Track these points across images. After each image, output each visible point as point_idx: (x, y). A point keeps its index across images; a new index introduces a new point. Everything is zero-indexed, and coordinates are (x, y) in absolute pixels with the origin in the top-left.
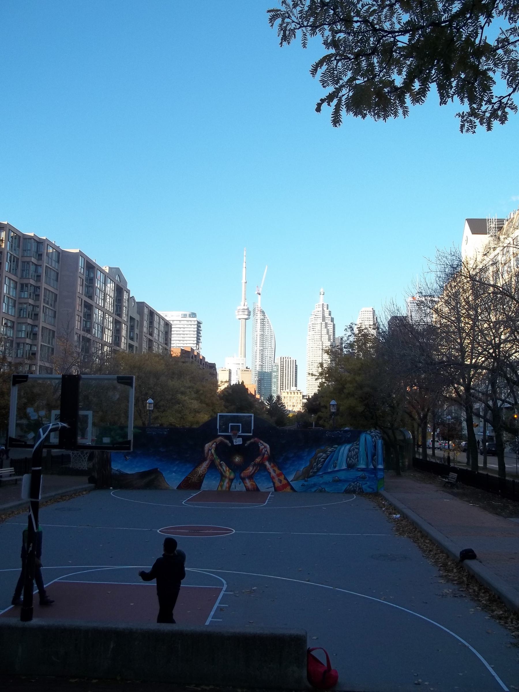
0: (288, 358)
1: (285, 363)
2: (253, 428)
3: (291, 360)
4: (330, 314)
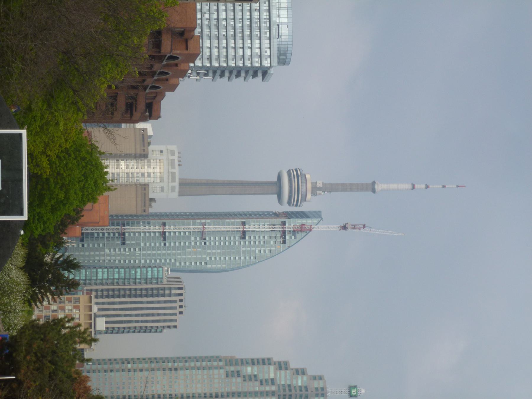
0: (181, 307)
3: (175, 314)
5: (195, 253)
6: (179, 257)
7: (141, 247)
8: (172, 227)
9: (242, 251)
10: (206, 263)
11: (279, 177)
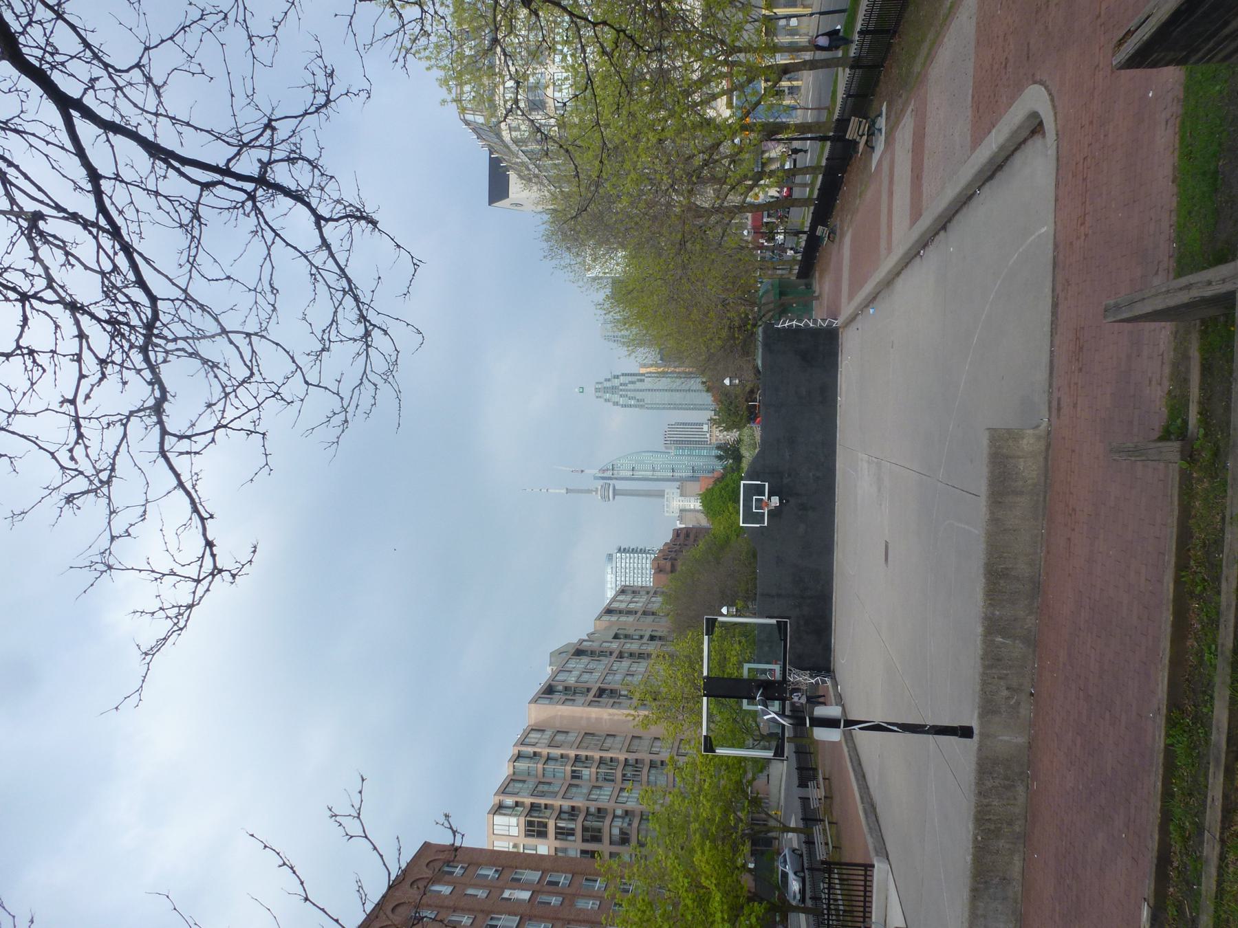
2: (759, 483)
4: (609, 380)
11: (614, 498)
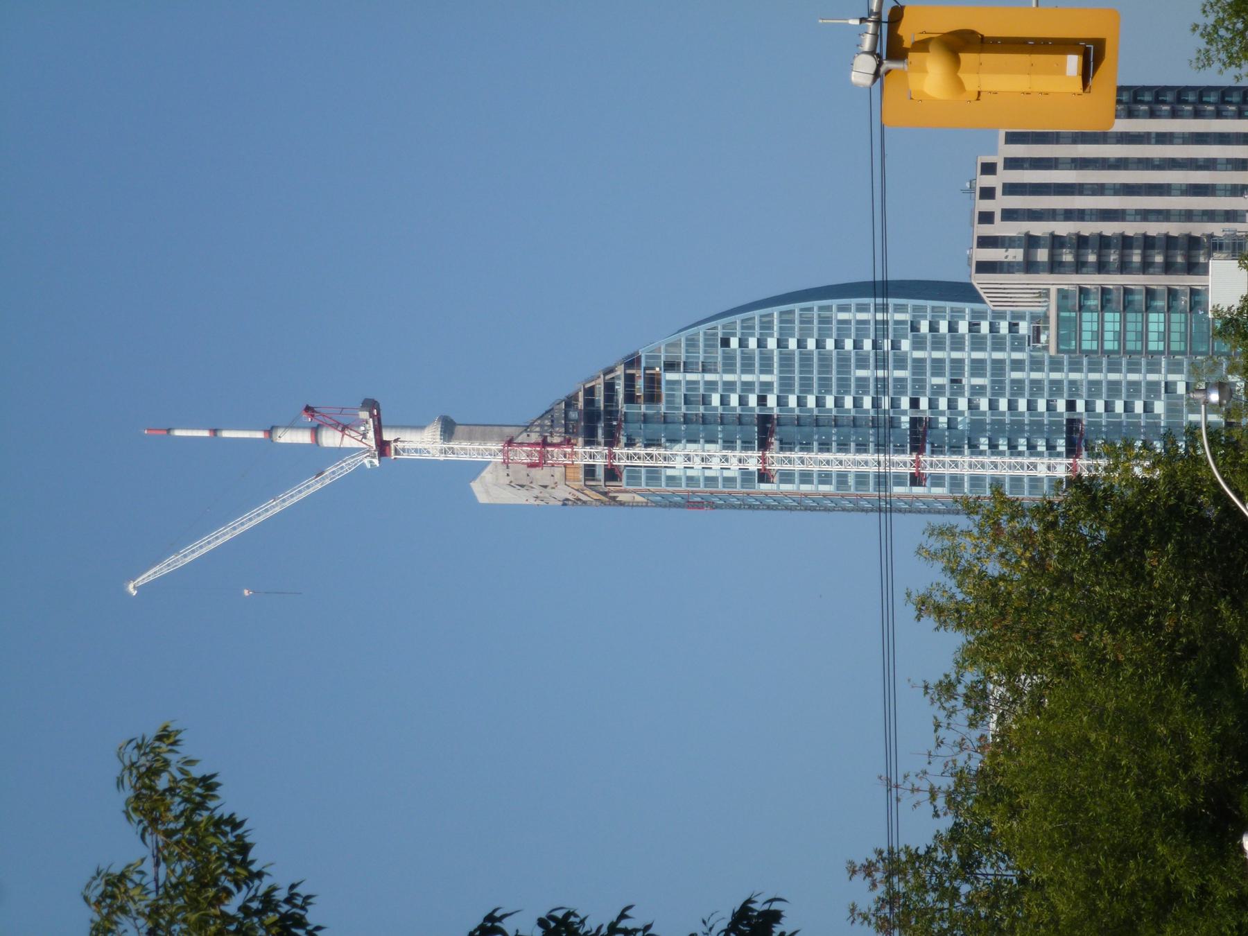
0: (988, 193)
1: (1039, 229)
3: (1012, 163)
5: (958, 364)
6: (1017, 356)
7: (1163, 396)
8: (1042, 472)
9: (771, 372)
10: (915, 328)
